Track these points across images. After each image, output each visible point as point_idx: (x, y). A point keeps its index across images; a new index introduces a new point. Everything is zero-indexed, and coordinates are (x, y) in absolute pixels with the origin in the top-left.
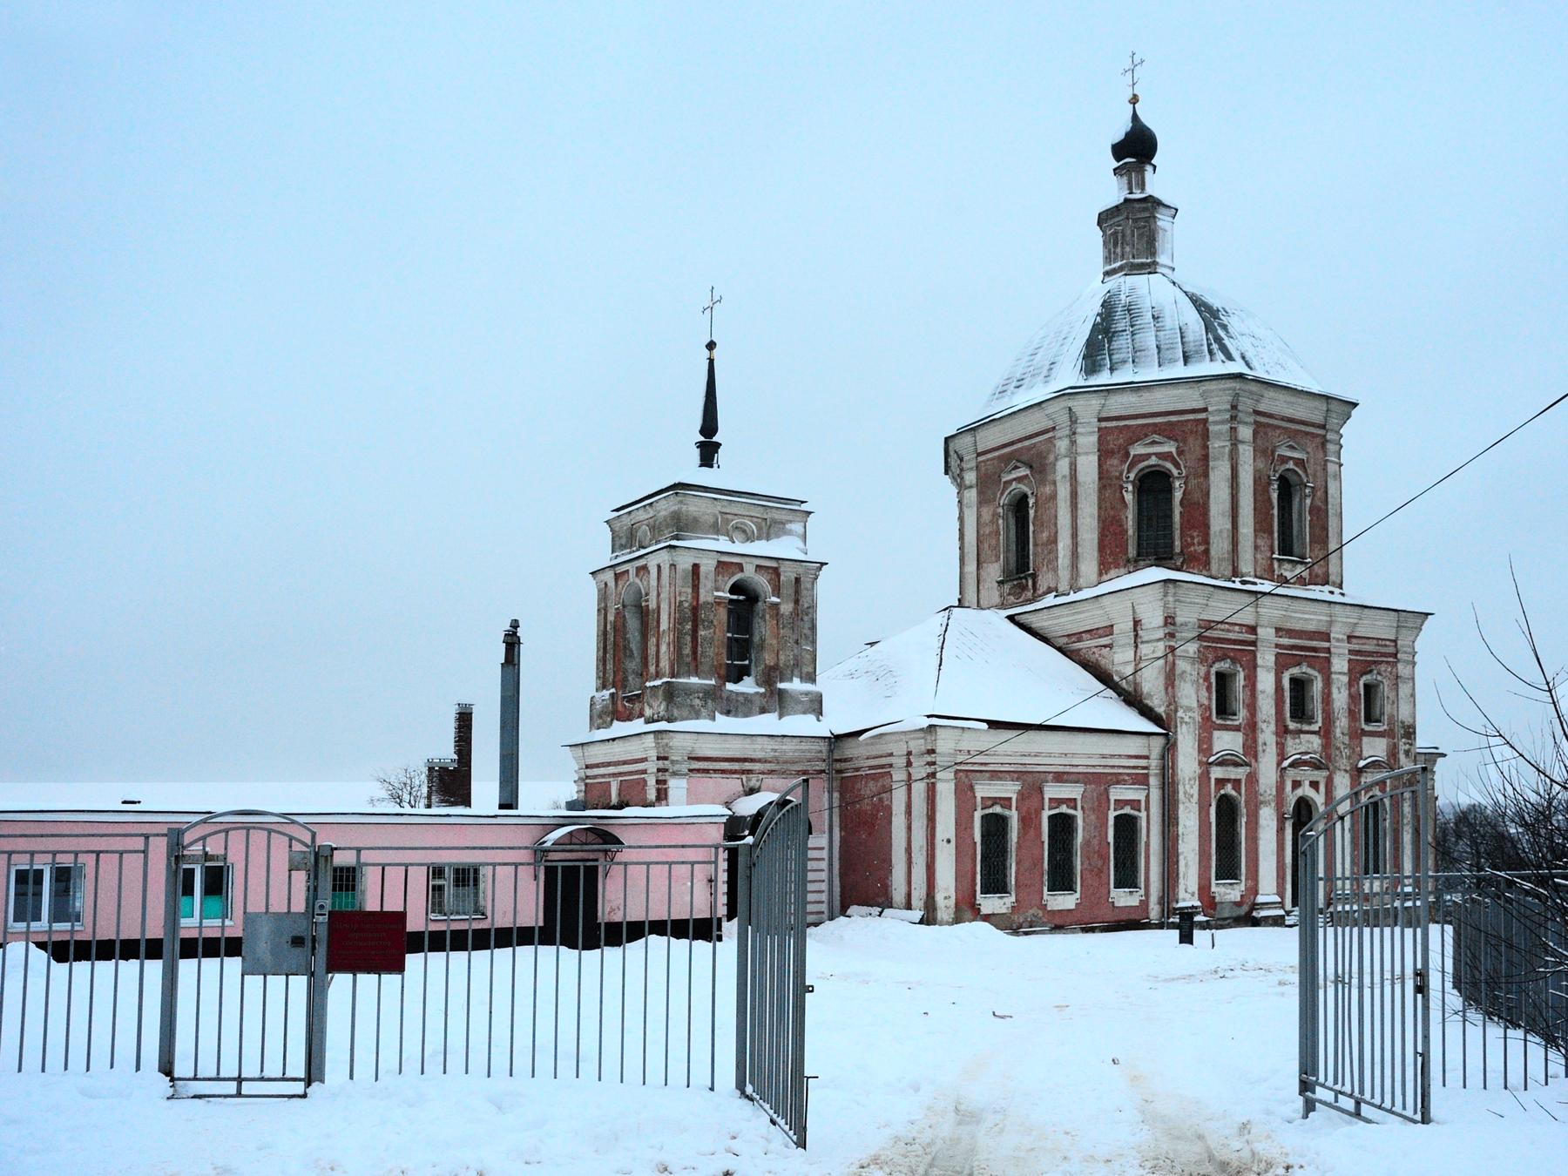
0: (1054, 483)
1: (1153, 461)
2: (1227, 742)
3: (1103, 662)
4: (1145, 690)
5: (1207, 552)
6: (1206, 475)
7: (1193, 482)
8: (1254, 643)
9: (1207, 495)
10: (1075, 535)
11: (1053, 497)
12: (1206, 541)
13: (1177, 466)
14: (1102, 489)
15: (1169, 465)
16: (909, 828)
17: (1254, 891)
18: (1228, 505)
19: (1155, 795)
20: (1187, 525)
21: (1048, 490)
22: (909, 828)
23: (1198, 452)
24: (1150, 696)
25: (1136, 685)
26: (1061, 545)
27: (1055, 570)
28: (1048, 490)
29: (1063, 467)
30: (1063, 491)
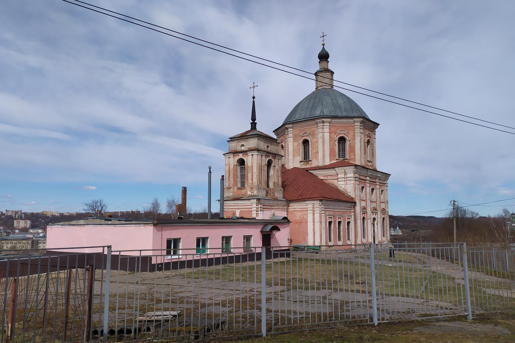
0: (318, 138)
1: (342, 135)
2: (363, 204)
3: (335, 184)
4: (348, 191)
5: (354, 158)
6: (354, 140)
7: (351, 141)
8: (366, 180)
9: (355, 144)
10: (324, 152)
11: (317, 142)
12: (354, 155)
13: (348, 136)
14: (330, 141)
15: (346, 137)
16: (314, 225)
17: (368, 240)
18: (360, 148)
19: (353, 216)
20: (350, 152)
21: (315, 140)
22: (314, 225)
23: (353, 134)
24: (350, 193)
25: (345, 190)
26: (319, 154)
27: (318, 160)
28: (315, 140)
29: (320, 135)
30: (320, 141)
